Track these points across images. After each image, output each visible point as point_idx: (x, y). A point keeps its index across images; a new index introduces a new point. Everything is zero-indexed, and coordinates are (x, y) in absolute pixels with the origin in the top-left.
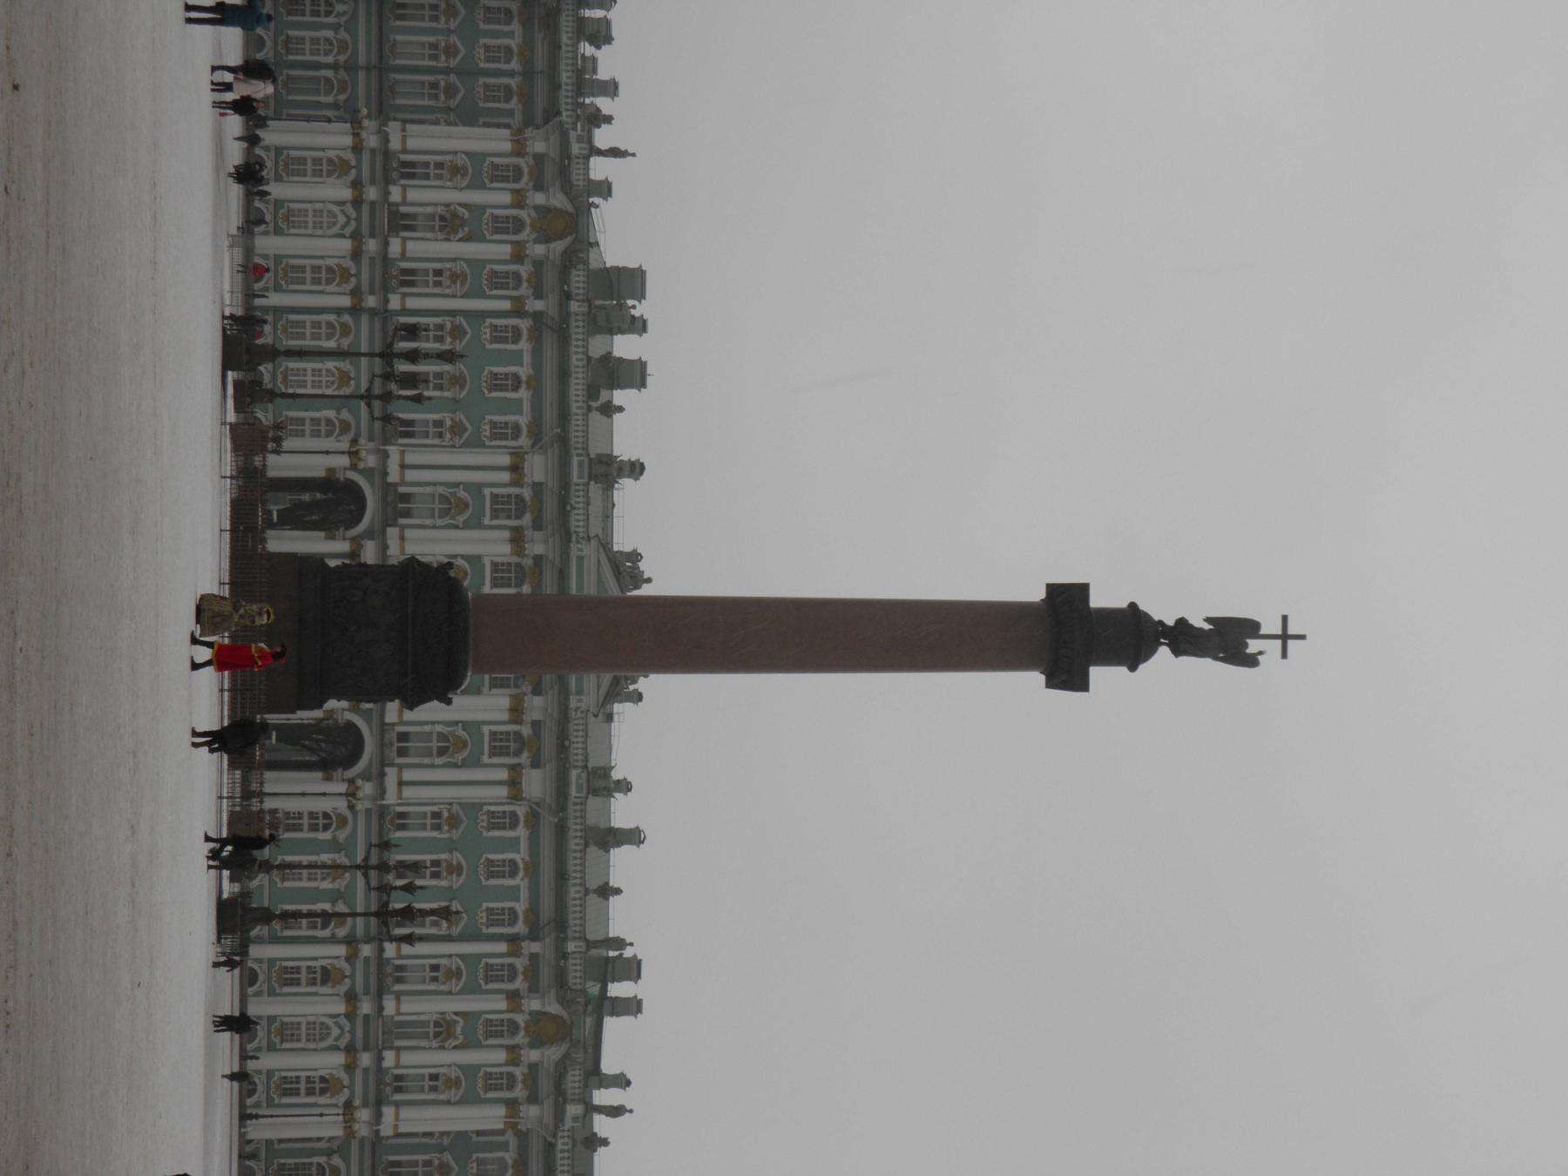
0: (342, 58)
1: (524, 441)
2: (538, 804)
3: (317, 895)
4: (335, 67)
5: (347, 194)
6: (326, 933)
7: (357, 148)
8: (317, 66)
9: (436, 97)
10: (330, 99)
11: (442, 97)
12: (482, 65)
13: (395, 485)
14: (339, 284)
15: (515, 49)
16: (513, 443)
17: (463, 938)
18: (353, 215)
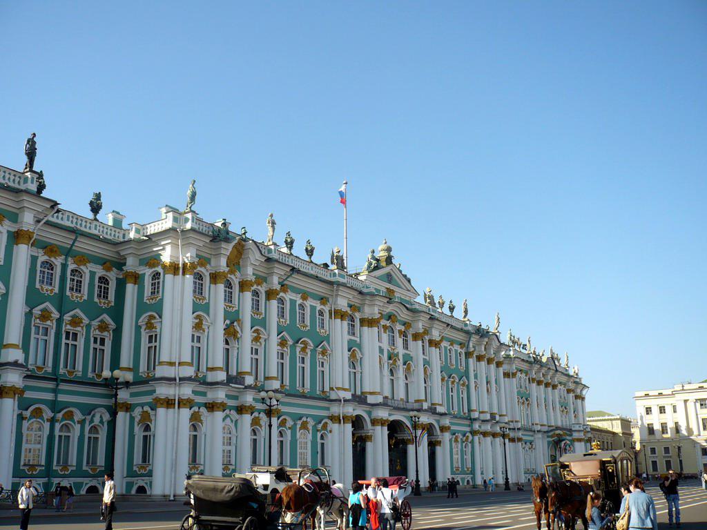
0: (48, 414)
1: (326, 309)
2: (440, 335)
3: (462, 450)
4: (52, 421)
5: (219, 415)
6: (470, 445)
7: (189, 403)
8: (51, 437)
9: (75, 335)
10: (78, 427)
11: (79, 329)
12: (56, 290)
13: (352, 395)
14: (261, 426)
15: (45, 258)
16: (327, 315)
17: (468, 378)
18: (227, 411)
